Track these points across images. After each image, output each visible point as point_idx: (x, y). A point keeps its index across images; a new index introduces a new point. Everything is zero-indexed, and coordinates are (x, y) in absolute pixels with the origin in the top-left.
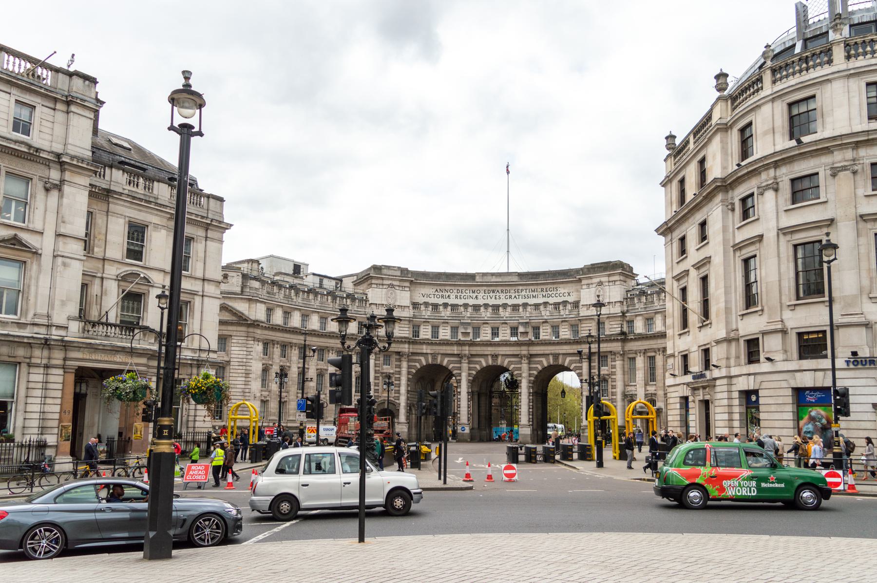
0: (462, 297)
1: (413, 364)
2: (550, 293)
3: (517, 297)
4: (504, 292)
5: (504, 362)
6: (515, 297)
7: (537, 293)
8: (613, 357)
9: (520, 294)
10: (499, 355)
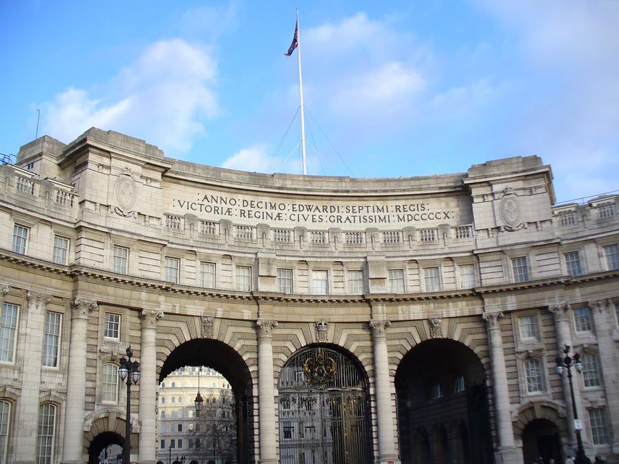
0: (253, 213)
3: (352, 219)
4: (328, 210)
6: (348, 219)
7: (386, 213)
8: (547, 317)
9: (358, 214)
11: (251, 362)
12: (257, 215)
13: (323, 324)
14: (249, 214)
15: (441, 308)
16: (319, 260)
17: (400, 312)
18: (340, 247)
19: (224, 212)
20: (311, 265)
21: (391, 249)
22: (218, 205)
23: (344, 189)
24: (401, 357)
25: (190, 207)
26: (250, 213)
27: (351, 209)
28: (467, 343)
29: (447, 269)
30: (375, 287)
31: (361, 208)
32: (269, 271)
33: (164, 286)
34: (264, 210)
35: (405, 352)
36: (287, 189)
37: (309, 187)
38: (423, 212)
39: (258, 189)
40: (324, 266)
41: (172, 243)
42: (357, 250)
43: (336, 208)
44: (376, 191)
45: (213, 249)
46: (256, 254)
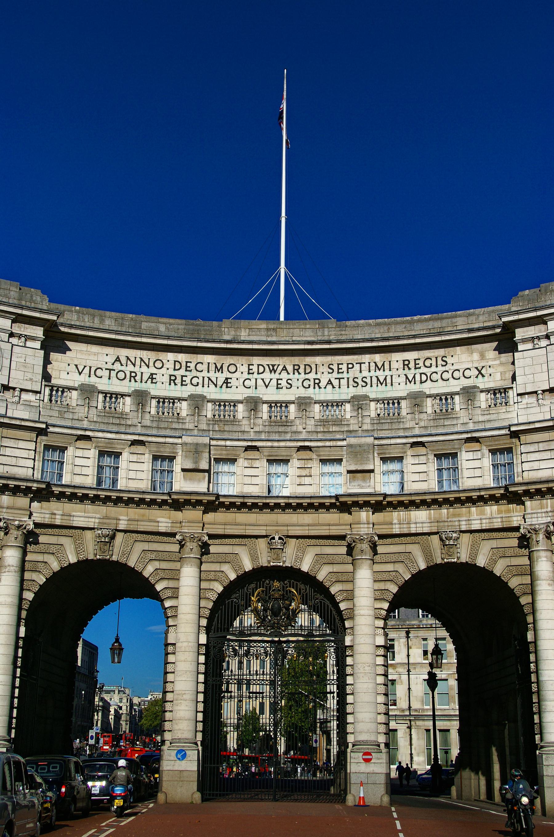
0: (188, 380)
1: (40, 558)
2: (428, 371)
3: (336, 383)
4: (301, 370)
5: (301, 560)
6: (330, 382)
7: (387, 372)
10: (288, 537)
11: (169, 593)
12: (195, 381)
13: (277, 538)
14: (182, 381)
15: (459, 515)
16: (276, 444)
17: (395, 521)
18: (311, 425)
19: (145, 377)
20: (266, 452)
21: (386, 426)
22: (137, 369)
23: (326, 338)
24: (394, 589)
25: (92, 372)
26: (184, 379)
27: (335, 367)
28: (498, 571)
29: (470, 455)
30: (356, 483)
31: (350, 366)
32: (196, 462)
33: (35, 486)
34: (205, 374)
35: (400, 583)
36: (243, 342)
37: (274, 339)
38: (444, 369)
39: (194, 344)
40: (283, 454)
41: (54, 426)
42: (335, 429)
43: (313, 367)
44: (372, 340)
45: (117, 433)
46: (181, 437)
